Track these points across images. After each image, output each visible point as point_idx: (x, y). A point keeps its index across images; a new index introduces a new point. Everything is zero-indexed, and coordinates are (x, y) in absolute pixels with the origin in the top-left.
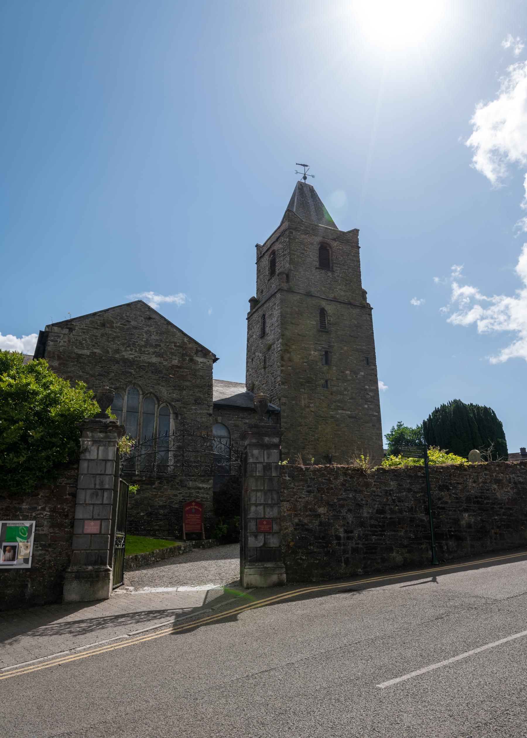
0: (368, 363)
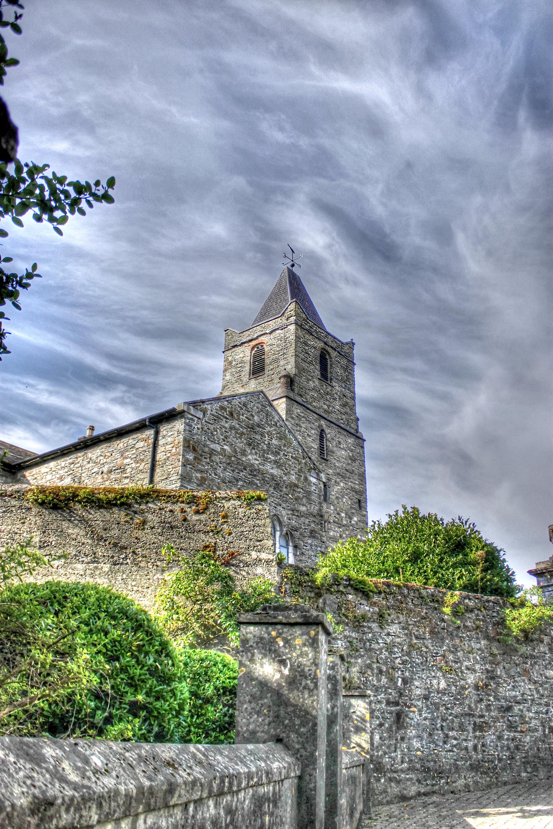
0: (360, 507)
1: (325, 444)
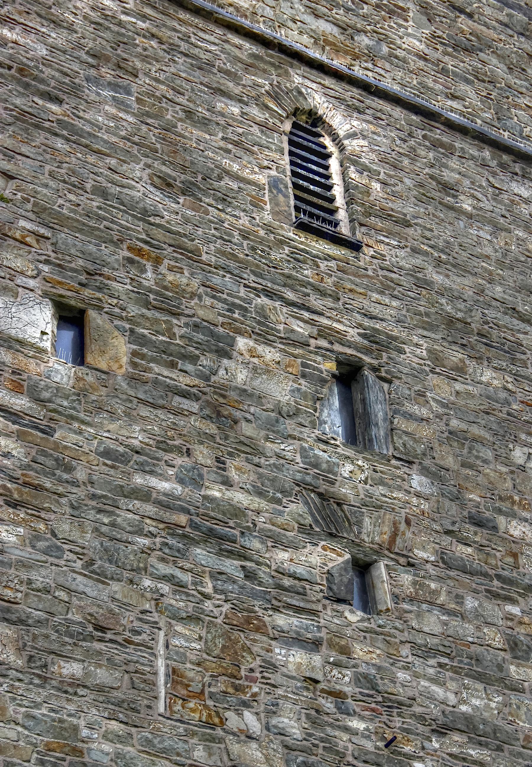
1: (336, 179)
